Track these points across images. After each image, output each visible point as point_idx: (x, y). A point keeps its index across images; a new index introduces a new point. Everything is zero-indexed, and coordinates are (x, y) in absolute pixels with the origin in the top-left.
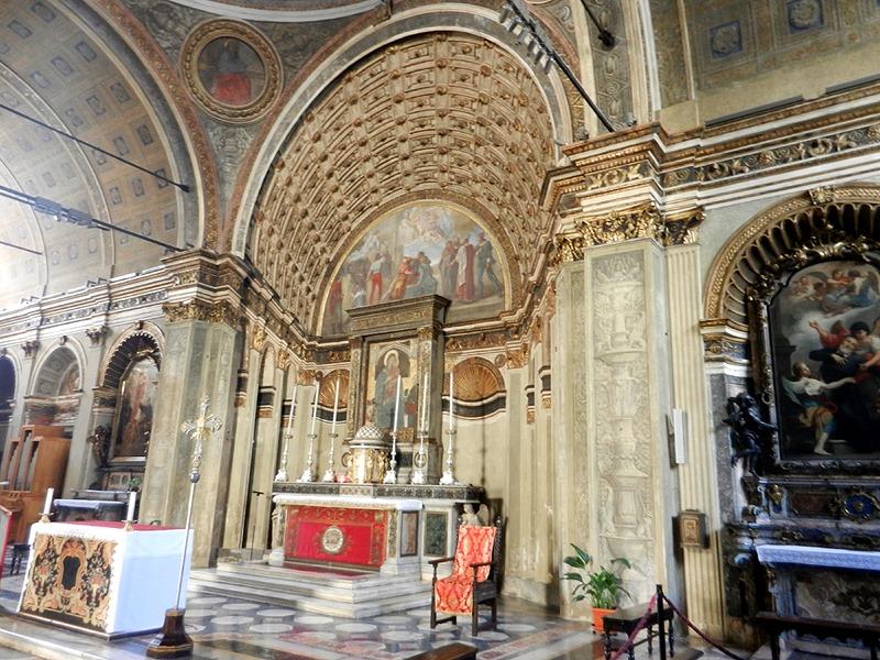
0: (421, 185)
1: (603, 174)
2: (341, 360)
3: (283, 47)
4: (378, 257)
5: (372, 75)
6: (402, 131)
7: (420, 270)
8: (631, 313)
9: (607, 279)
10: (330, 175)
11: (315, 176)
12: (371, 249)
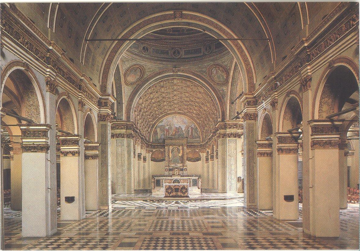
4: (167, 125)
6: (175, 98)
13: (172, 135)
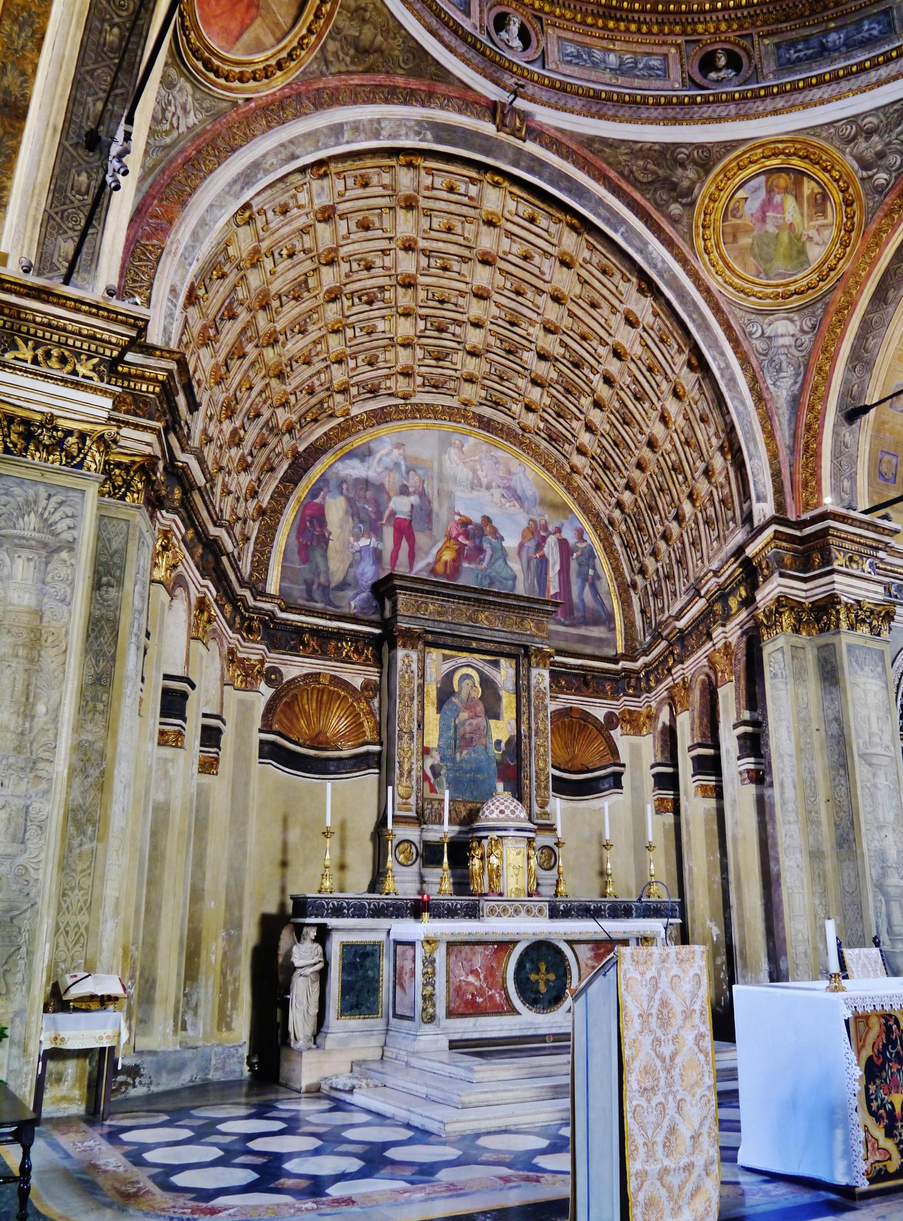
1: (845, 554)
2: (323, 654)
4: (404, 491)
5: (451, 190)
6: (476, 309)
7: (486, 545)
8: (881, 714)
9: (860, 672)
10: (334, 296)
12: (386, 468)
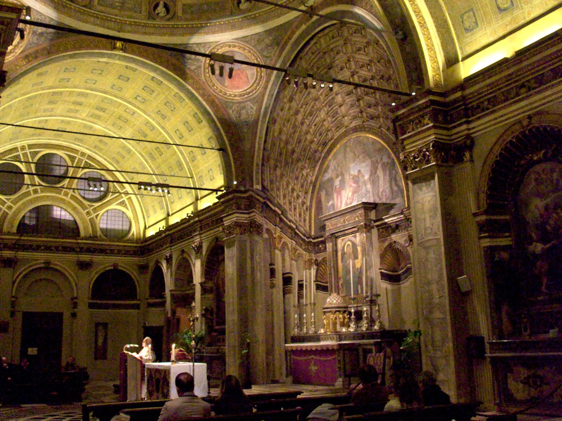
0: (353, 122)
3: (259, 48)
4: (337, 177)
11: (295, 126)
13: (347, 204)
